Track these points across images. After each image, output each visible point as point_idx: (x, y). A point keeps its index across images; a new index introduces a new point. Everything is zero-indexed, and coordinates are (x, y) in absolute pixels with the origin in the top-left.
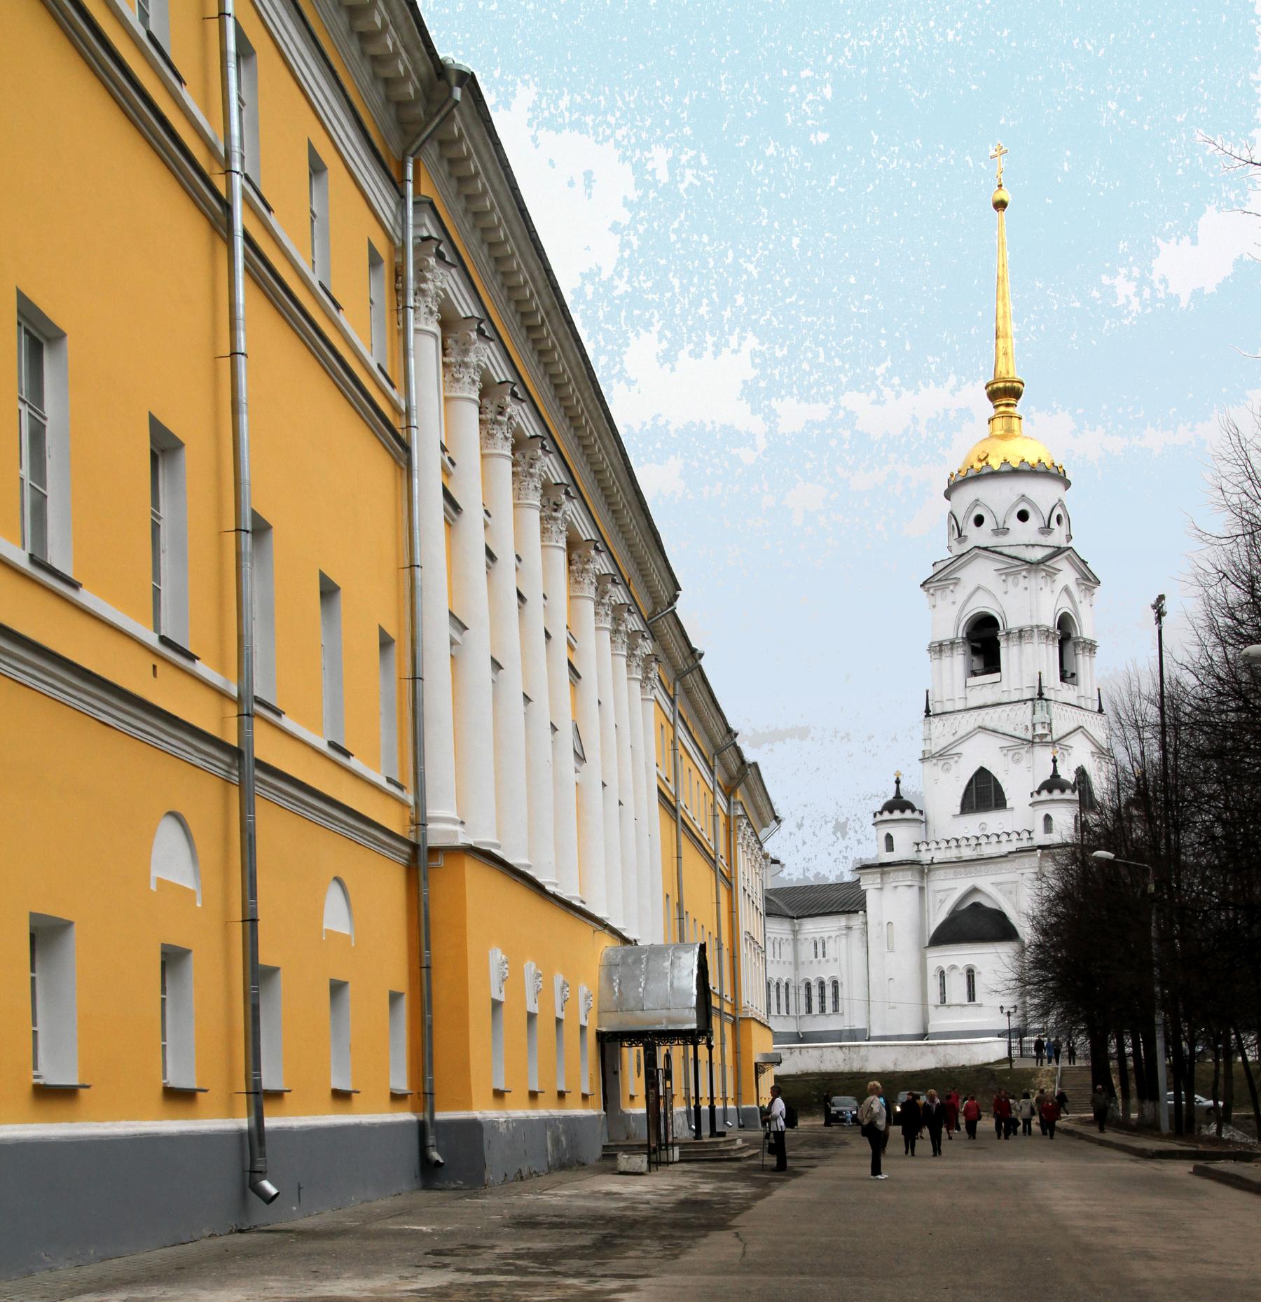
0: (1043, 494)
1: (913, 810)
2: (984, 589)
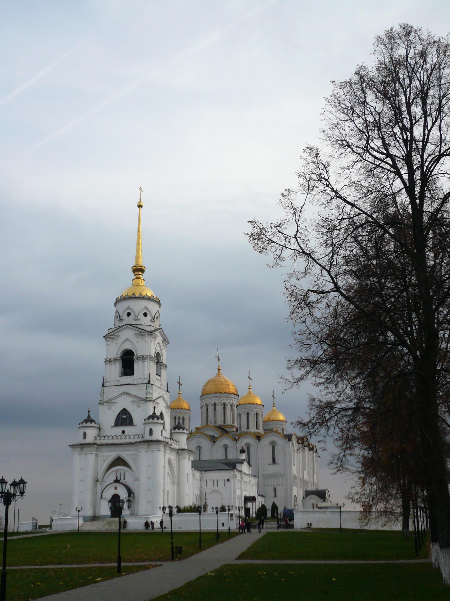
0: (153, 308)
2: (127, 340)
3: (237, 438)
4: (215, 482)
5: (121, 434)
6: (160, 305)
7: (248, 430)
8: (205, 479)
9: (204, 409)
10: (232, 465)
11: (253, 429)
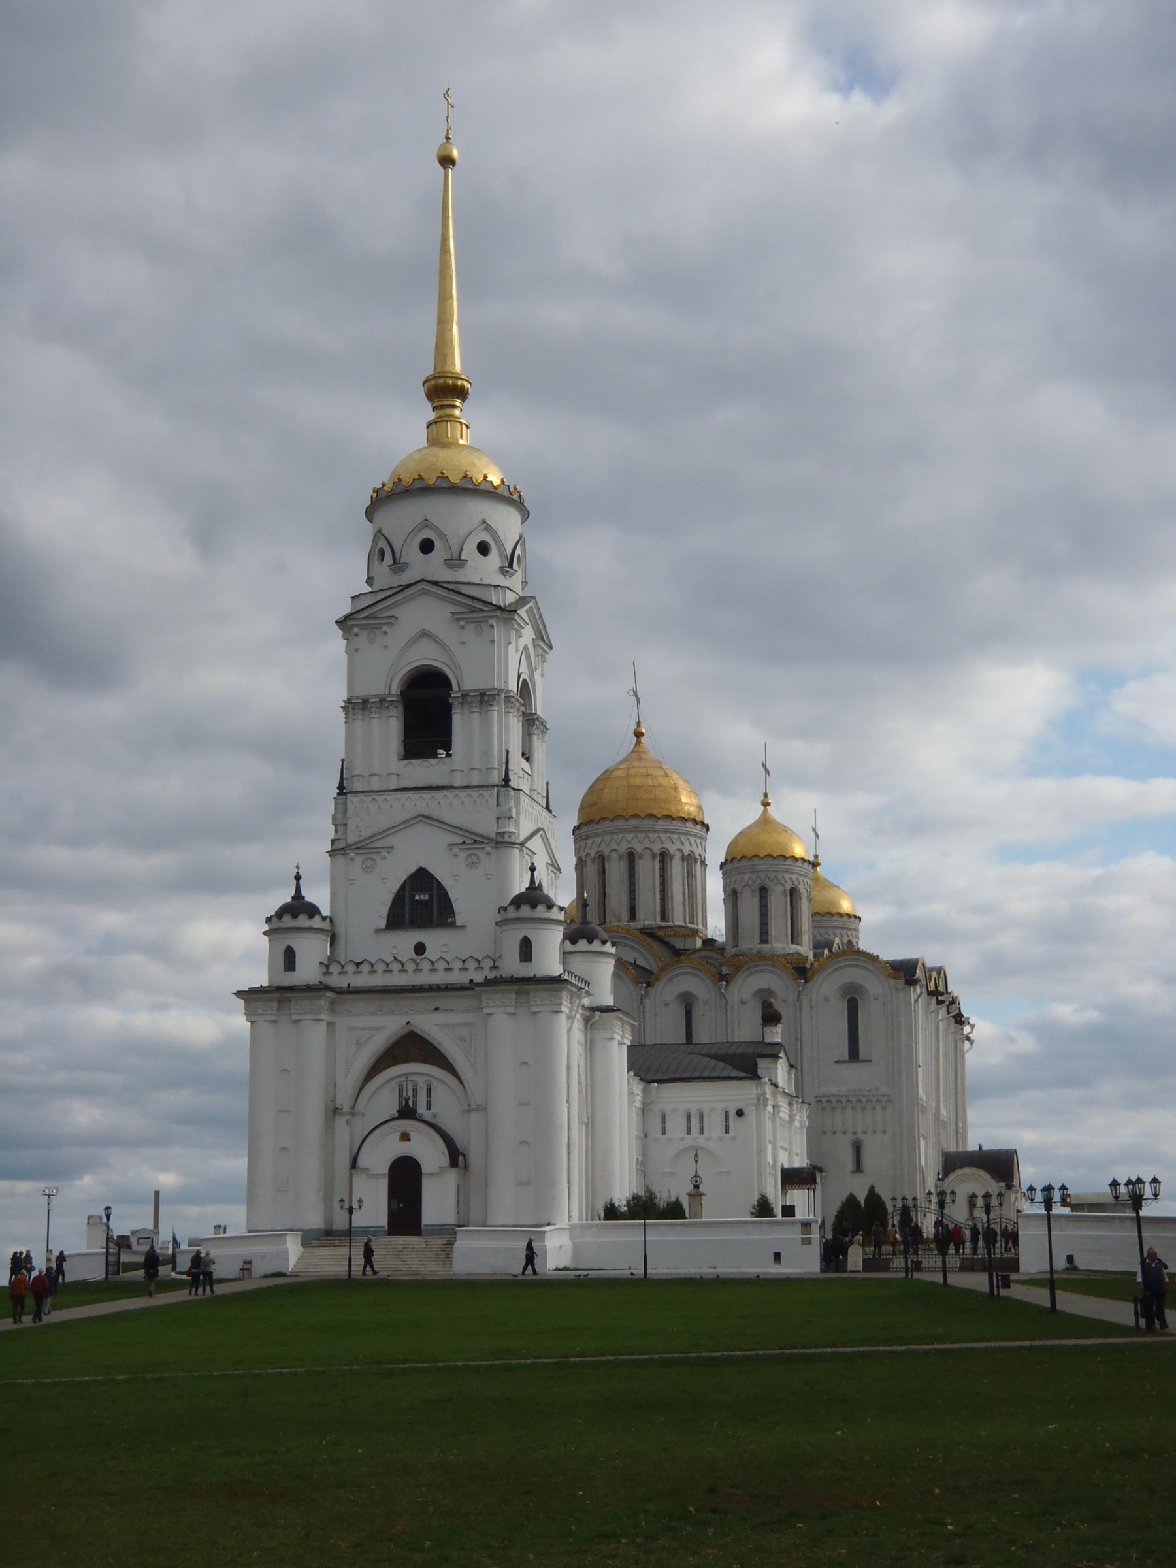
0: (507, 524)
1: (324, 918)
3: (725, 970)
4: (695, 1121)
5: (414, 956)
6: (525, 514)
7: (764, 946)
8: (657, 1109)
9: (592, 870)
10: (745, 1064)
11: (780, 944)
